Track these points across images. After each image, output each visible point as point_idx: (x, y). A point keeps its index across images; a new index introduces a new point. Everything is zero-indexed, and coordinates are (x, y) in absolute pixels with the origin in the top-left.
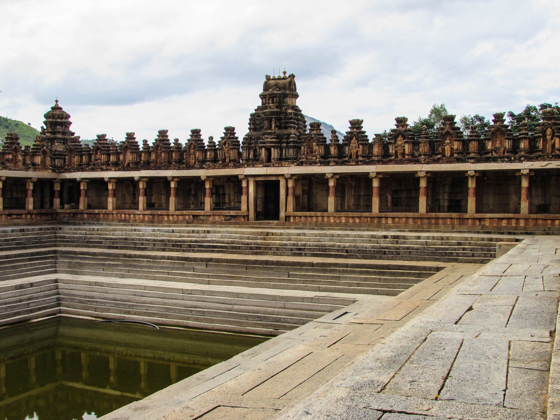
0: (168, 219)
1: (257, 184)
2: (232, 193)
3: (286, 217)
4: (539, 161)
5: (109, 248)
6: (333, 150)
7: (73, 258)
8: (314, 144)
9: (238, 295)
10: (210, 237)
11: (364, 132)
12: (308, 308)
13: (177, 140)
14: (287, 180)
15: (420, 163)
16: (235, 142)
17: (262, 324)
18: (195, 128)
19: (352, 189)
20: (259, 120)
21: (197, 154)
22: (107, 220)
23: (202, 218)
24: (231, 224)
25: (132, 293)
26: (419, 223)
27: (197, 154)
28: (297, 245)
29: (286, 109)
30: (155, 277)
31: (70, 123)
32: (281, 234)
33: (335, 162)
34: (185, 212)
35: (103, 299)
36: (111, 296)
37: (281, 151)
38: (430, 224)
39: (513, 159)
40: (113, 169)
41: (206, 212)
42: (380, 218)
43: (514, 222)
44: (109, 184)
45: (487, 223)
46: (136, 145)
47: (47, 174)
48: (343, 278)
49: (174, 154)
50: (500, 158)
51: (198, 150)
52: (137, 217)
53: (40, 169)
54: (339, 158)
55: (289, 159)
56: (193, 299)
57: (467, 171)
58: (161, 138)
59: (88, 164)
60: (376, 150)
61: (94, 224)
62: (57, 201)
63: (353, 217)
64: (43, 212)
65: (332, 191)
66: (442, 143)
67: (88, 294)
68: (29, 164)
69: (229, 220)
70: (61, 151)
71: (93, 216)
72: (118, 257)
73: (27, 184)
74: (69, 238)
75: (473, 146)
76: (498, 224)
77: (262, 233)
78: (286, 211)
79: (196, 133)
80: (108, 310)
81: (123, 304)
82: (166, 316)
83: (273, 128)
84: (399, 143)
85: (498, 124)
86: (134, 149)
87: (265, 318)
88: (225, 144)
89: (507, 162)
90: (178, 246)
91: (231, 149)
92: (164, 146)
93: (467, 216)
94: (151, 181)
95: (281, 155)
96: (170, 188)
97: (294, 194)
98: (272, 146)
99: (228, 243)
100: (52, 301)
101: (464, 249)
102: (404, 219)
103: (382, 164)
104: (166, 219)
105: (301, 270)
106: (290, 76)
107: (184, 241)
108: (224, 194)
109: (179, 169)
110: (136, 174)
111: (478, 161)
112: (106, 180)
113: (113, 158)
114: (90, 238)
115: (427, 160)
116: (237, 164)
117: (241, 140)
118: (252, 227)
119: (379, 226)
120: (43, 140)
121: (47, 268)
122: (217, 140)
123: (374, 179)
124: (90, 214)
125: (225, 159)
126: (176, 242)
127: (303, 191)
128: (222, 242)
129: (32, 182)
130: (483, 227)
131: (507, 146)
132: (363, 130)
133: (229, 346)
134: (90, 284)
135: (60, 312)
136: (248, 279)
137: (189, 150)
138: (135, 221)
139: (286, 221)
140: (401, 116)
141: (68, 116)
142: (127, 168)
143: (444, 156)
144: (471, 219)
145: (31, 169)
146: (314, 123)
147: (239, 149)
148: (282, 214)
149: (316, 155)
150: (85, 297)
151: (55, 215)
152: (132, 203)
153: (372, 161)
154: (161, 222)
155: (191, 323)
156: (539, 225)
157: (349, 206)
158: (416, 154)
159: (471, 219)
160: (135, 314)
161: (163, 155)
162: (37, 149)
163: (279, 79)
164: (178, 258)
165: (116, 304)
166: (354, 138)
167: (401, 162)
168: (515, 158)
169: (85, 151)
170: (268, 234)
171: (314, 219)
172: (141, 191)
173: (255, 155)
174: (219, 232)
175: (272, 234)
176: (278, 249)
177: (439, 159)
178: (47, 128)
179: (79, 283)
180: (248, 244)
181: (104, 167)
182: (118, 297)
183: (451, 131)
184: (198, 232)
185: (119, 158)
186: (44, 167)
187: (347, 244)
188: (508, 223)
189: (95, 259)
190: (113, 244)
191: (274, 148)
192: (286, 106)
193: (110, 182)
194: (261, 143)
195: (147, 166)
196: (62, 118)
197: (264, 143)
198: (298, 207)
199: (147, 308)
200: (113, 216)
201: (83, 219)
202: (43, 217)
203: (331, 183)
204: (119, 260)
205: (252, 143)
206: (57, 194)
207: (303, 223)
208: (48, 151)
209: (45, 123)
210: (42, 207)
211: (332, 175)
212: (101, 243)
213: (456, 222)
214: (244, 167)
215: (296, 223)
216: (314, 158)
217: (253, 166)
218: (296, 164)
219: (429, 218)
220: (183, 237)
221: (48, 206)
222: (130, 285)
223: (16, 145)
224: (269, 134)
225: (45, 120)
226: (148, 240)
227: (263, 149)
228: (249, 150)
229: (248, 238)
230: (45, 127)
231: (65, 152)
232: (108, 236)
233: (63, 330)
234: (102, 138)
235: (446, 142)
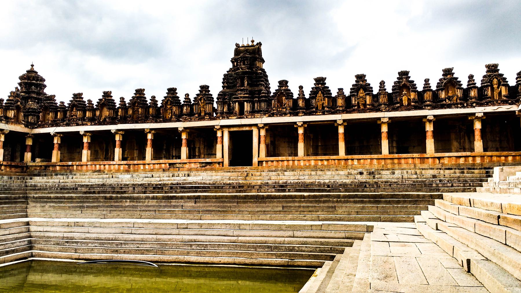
0: (144, 168)
1: (230, 133)
2: (202, 147)
3: (259, 162)
4: (490, 106)
5: (85, 193)
6: (301, 103)
7: (47, 202)
8: (284, 98)
10: (190, 179)
11: (328, 87)
12: (320, 236)
13: (153, 97)
14: (259, 129)
15: (382, 111)
16: (210, 97)
17: (275, 254)
18: (172, 87)
19: (310, 140)
20: (231, 79)
21: (174, 109)
22: (81, 171)
23: (178, 165)
24: (206, 170)
25: (120, 231)
26: (383, 163)
27: (174, 109)
29: (256, 70)
31: (45, 86)
33: (303, 112)
34: (161, 161)
35: (84, 239)
37: (254, 106)
38: (393, 163)
39: (465, 105)
42: (345, 160)
43: (470, 159)
45: (446, 161)
46: (113, 102)
47: (20, 128)
48: (339, 207)
49: (151, 110)
50: (454, 105)
51: (175, 106)
52: (112, 167)
53: (12, 123)
54: (306, 110)
56: (190, 233)
57: (425, 117)
58: (138, 95)
59: (63, 120)
62: (28, 156)
64: (13, 164)
65: (301, 138)
66: (400, 94)
67: (66, 235)
69: (204, 167)
70: (35, 109)
71: (66, 168)
75: (428, 96)
76: (456, 161)
78: (259, 157)
79: (172, 91)
81: (109, 243)
82: (163, 253)
83: (246, 85)
84: (361, 95)
85: (448, 76)
86: (111, 105)
87: (276, 248)
88: (200, 100)
89: (460, 108)
90: (159, 188)
91: (207, 103)
92: (142, 102)
93: (426, 156)
95: (253, 107)
96: (147, 140)
98: (246, 101)
99: (210, 184)
100: (23, 244)
101: (440, 181)
102: (369, 160)
103: (346, 113)
104: (142, 167)
105: (294, 202)
106: (257, 44)
107: (164, 184)
108: (194, 149)
109: (156, 122)
110: (113, 128)
111: (434, 108)
112: (82, 133)
113: (88, 114)
114: (64, 186)
115: (387, 108)
116: (212, 118)
117: (215, 96)
119: (346, 167)
120: (18, 96)
121: (17, 212)
122: (192, 97)
123: (340, 127)
124: (64, 166)
125: (201, 113)
126: (156, 185)
127: (271, 141)
128: (205, 183)
129: (3, 134)
130: (443, 164)
131: (459, 95)
133: (232, 282)
135: (32, 256)
137: (166, 106)
139: (259, 165)
140: (359, 73)
141: (43, 80)
142: (104, 123)
143: (402, 105)
144: (431, 158)
146: (283, 81)
147: (213, 104)
148: (255, 160)
149: (286, 108)
150: (63, 238)
152: (105, 158)
155: (193, 258)
156: (494, 161)
158: (376, 104)
159: (431, 158)
160: (124, 252)
161: (140, 110)
162: (11, 103)
164: (164, 198)
165: (100, 243)
166: (320, 92)
167: (364, 111)
168: (467, 105)
171: (286, 163)
172: (117, 143)
173: (229, 109)
176: (260, 187)
177: (398, 107)
178: (22, 88)
179: (54, 225)
180: (230, 184)
182: (103, 236)
183: (408, 84)
185: (95, 114)
186: (16, 121)
187: (327, 181)
188: (465, 161)
189: (71, 202)
191: (247, 103)
192: (256, 67)
193: (85, 136)
194: (235, 98)
195: (124, 120)
196: (37, 81)
197: (238, 98)
198: (268, 154)
199: (138, 246)
201: (55, 171)
203: (301, 131)
204: (100, 202)
205: (227, 99)
206: (28, 149)
207: (275, 166)
208: (22, 107)
209: (20, 84)
210: (12, 159)
211: (302, 123)
213: (417, 161)
214: (219, 119)
216: (285, 110)
217: (228, 118)
218: (267, 115)
221: (18, 160)
222: (116, 223)
224: (241, 90)
225: (19, 81)
226: (127, 185)
227: (237, 103)
228: (223, 104)
229: (229, 179)
230: (19, 88)
231: (40, 109)
232: (83, 184)
233: (35, 278)
234: (78, 96)
235: (403, 93)
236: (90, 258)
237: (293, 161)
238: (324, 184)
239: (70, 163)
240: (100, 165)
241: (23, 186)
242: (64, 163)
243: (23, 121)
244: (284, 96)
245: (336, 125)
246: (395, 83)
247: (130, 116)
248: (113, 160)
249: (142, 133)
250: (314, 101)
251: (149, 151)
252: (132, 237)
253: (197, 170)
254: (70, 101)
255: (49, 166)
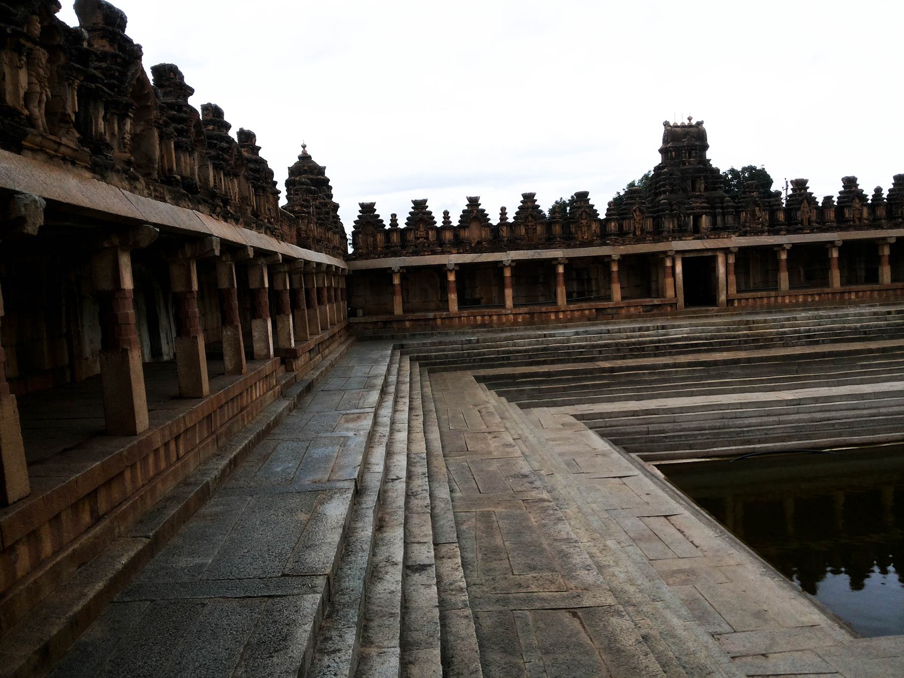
0: (557, 317)
1: (685, 262)
3: (728, 301)
9: (862, 396)
10: (674, 333)
15: (882, 228)
24: (654, 315)
27: (594, 226)
28: (799, 332)
30: (693, 391)
32: (765, 321)
34: (584, 305)
36: (694, 425)
40: (454, 252)
41: (618, 303)
42: (842, 293)
44: (449, 274)
46: (482, 217)
52: (504, 319)
55: (728, 228)
60: (832, 215)
61: (432, 334)
63: (812, 295)
65: (783, 265)
71: (422, 323)
72: (591, 373)
74: (436, 357)
77: (740, 323)
80: (714, 445)
81: (727, 433)
84: (857, 206)
94: (518, 265)
95: (714, 222)
97: (736, 273)
102: (869, 293)
104: (553, 317)
109: (568, 246)
114: (479, 354)
118: (690, 318)
119: (843, 303)
126: (628, 344)
132: (808, 191)
134: (635, 413)
136: (819, 377)
138: (501, 324)
140: (849, 175)
142: (478, 248)
148: (723, 298)
153: (832, 227)
154: (545, 323)
157: (754, 284)
160: (759, 442)
161: (539, 228)
163: (683, 126)
164: (690, 364)
170: (747, 322)
171: (765, 301)
172: (508, 281)
173: (679, 226)
174: (679, 326)
175: (754, 322)
176: (781, 339)
177: (901, 223)
182: (706, 424)
184: (648, 329)
190: (532, 358)
194: (687, 209)
195: (514, 245)
197: (693, 209)
212: (508, 358)
215: (743, 308)
219: (895, 289)
220: (632, 337)
222: (703, 406)
224: (698, 197)
226: (583, 347)
229: (728, 330)
236: (723, 453)
237: (776, 297)
238: (856, 328)
239: (431, 315)
240: (483, 316)
244: (758, 205)
245: (828, 246)
246: (890, 190)
248: (503, 306)
249: (550, 264)
250: (799, 213)
251: (561, 291)
252: (747, 421)
253: (640, 316)
254: (410, 213)
255: (391, 322)
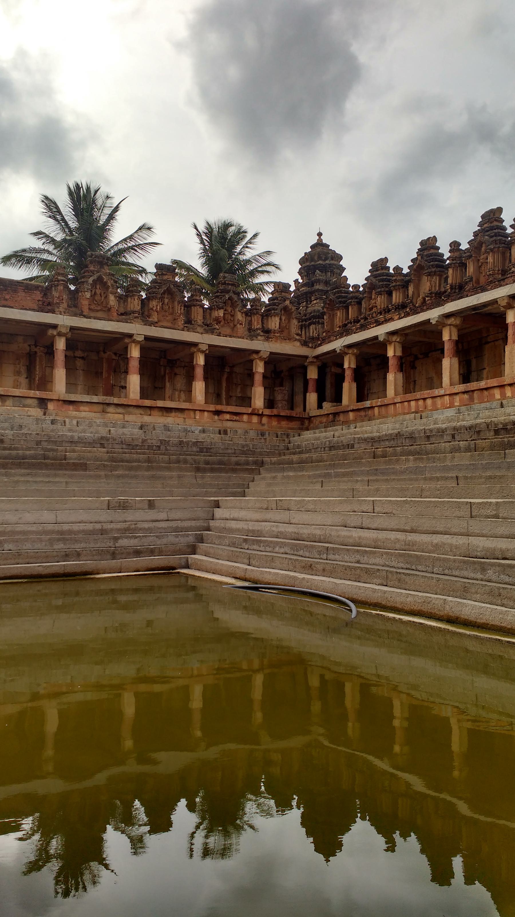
53: (277, 338)
59: (357, 321)
68: (257, 329)
71: (362, 413)
73: (254, 362)
110: (433, 314)
112: (381, 339)
124: (358, 410)
129: (261, 359)
145: (259, 338)
151: (307, 422)
169: (352, 298)
181: (381, 317)
200: (395, 408)
202: (284, 423)
206: (311, 386)
223: (231, 294)
241: (282, 447)
242: (360, 405)
243: (298, 334)
247: (471, 279)
